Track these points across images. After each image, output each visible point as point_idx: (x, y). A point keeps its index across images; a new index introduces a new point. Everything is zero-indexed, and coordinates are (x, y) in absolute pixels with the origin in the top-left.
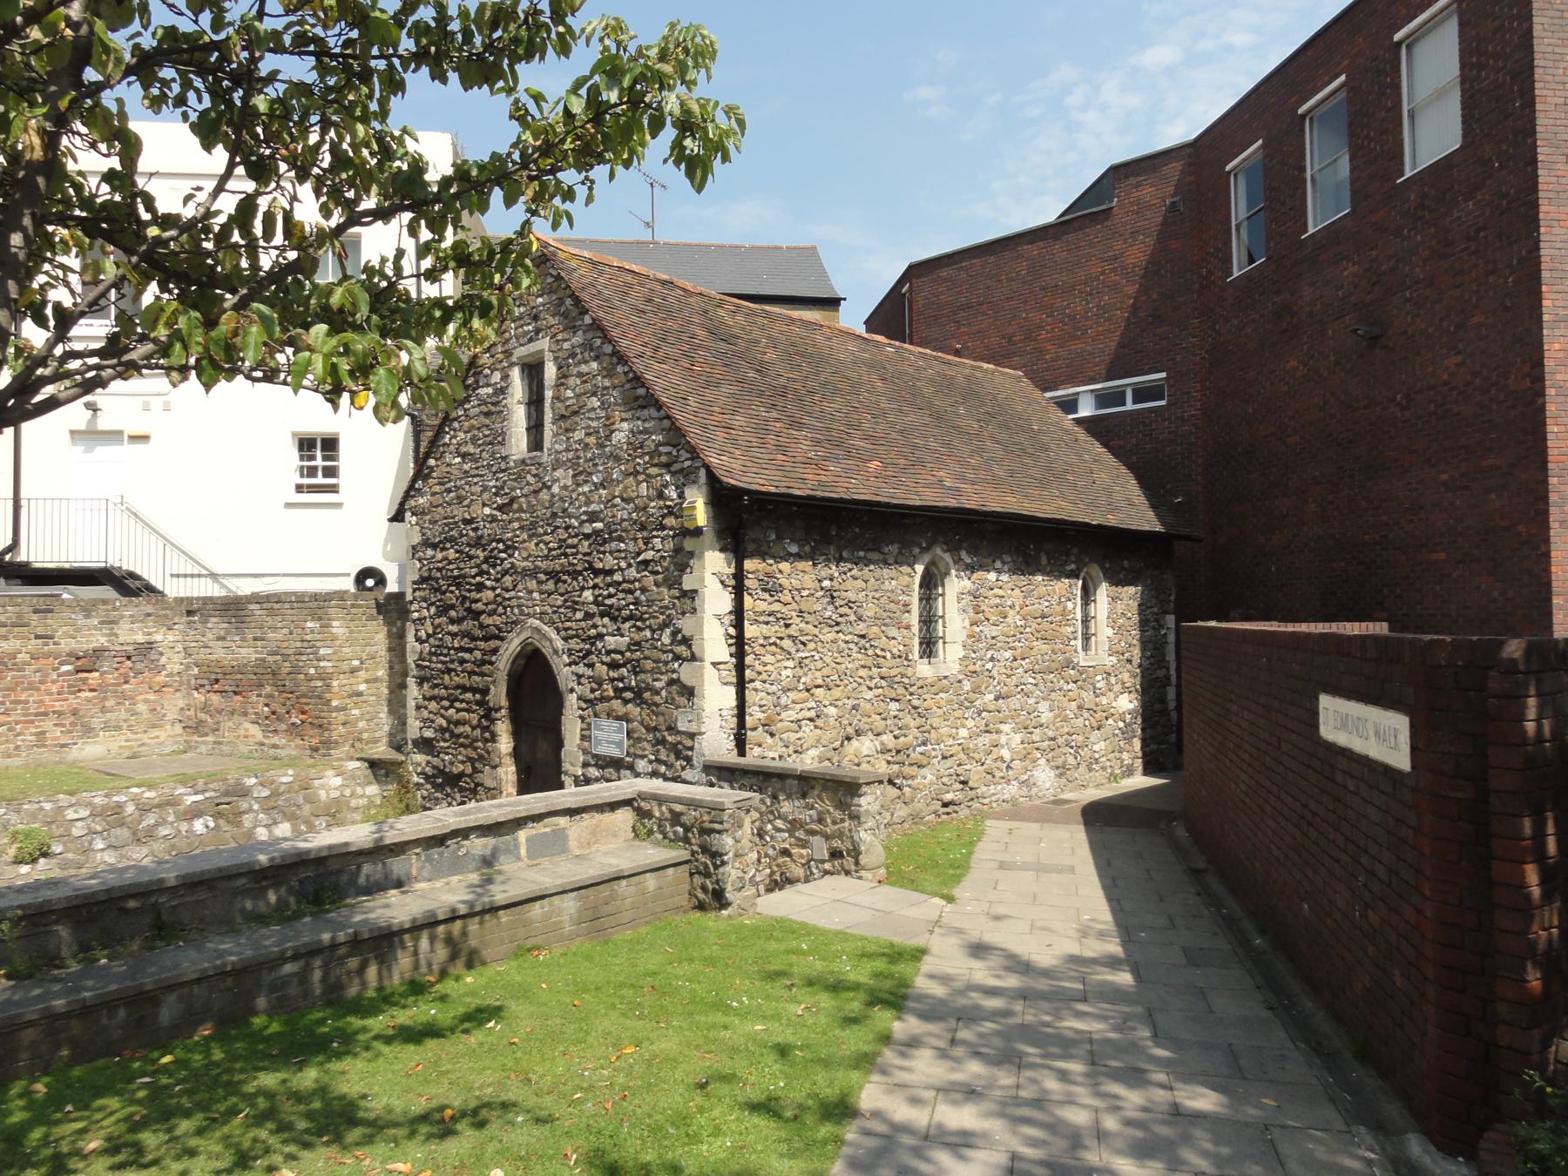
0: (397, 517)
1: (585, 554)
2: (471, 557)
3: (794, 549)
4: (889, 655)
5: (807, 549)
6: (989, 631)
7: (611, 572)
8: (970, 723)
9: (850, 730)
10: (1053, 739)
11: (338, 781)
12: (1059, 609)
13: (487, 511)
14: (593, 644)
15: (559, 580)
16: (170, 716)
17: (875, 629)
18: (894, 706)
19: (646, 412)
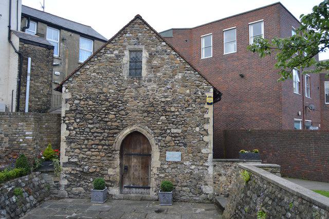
19: (189, 72)
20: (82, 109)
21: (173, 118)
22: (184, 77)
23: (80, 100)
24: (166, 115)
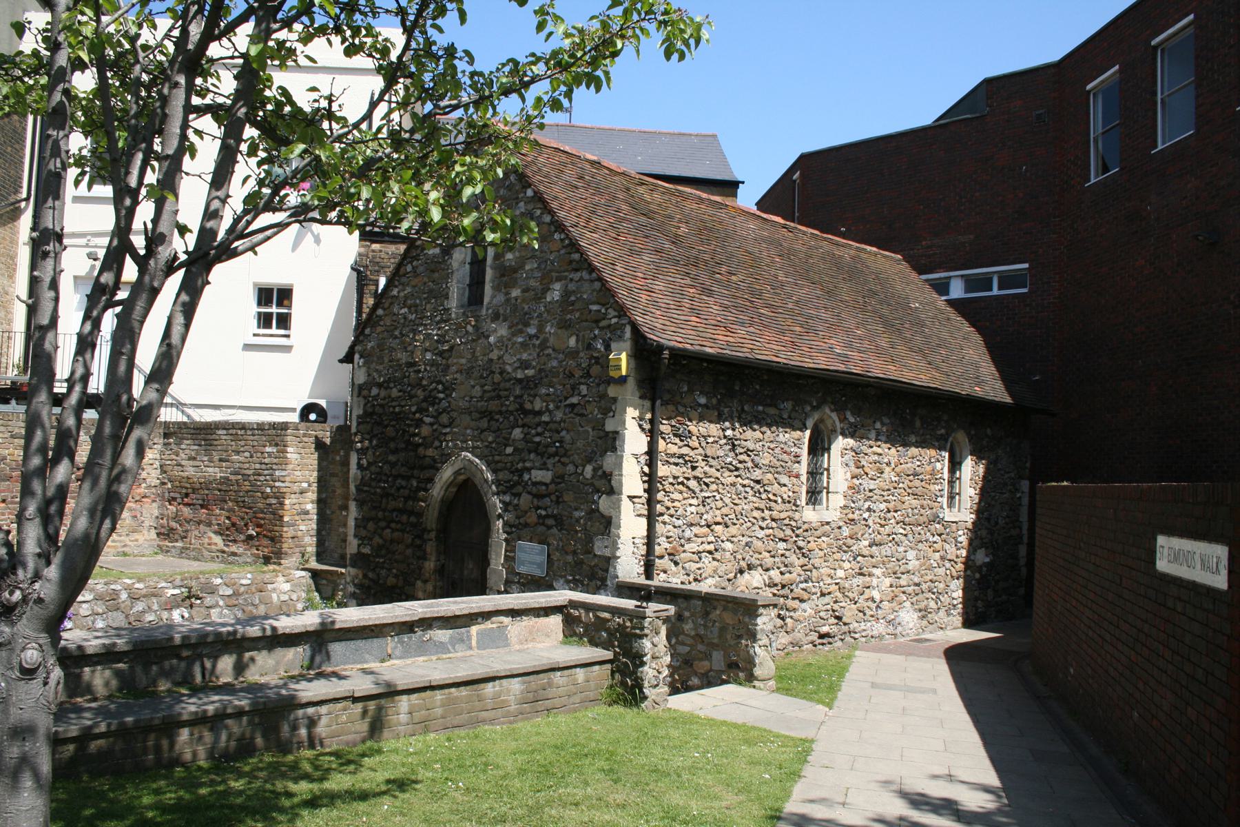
0: (348, 358)
1: (516, 397)
2: (411, 397)
3: (703, 400)
4: (780, 500)
5: (714, 401)
6: (867, 484)
7: (540, 413)
8: (846, 565)
9: (743, 564)
10: (917, 585)
11: (287, 587)
12: (929, 468)
13: (428, 356)
14: (521, 476)
15: (492, 419)
16: (147, 524)
17: (769, 476)
18: (782, 545)
19: (578, 274)
20: (381, 411)
21: (538, 434)
22: (566, 294)
23: (380, 386)
24: (523, 426)
